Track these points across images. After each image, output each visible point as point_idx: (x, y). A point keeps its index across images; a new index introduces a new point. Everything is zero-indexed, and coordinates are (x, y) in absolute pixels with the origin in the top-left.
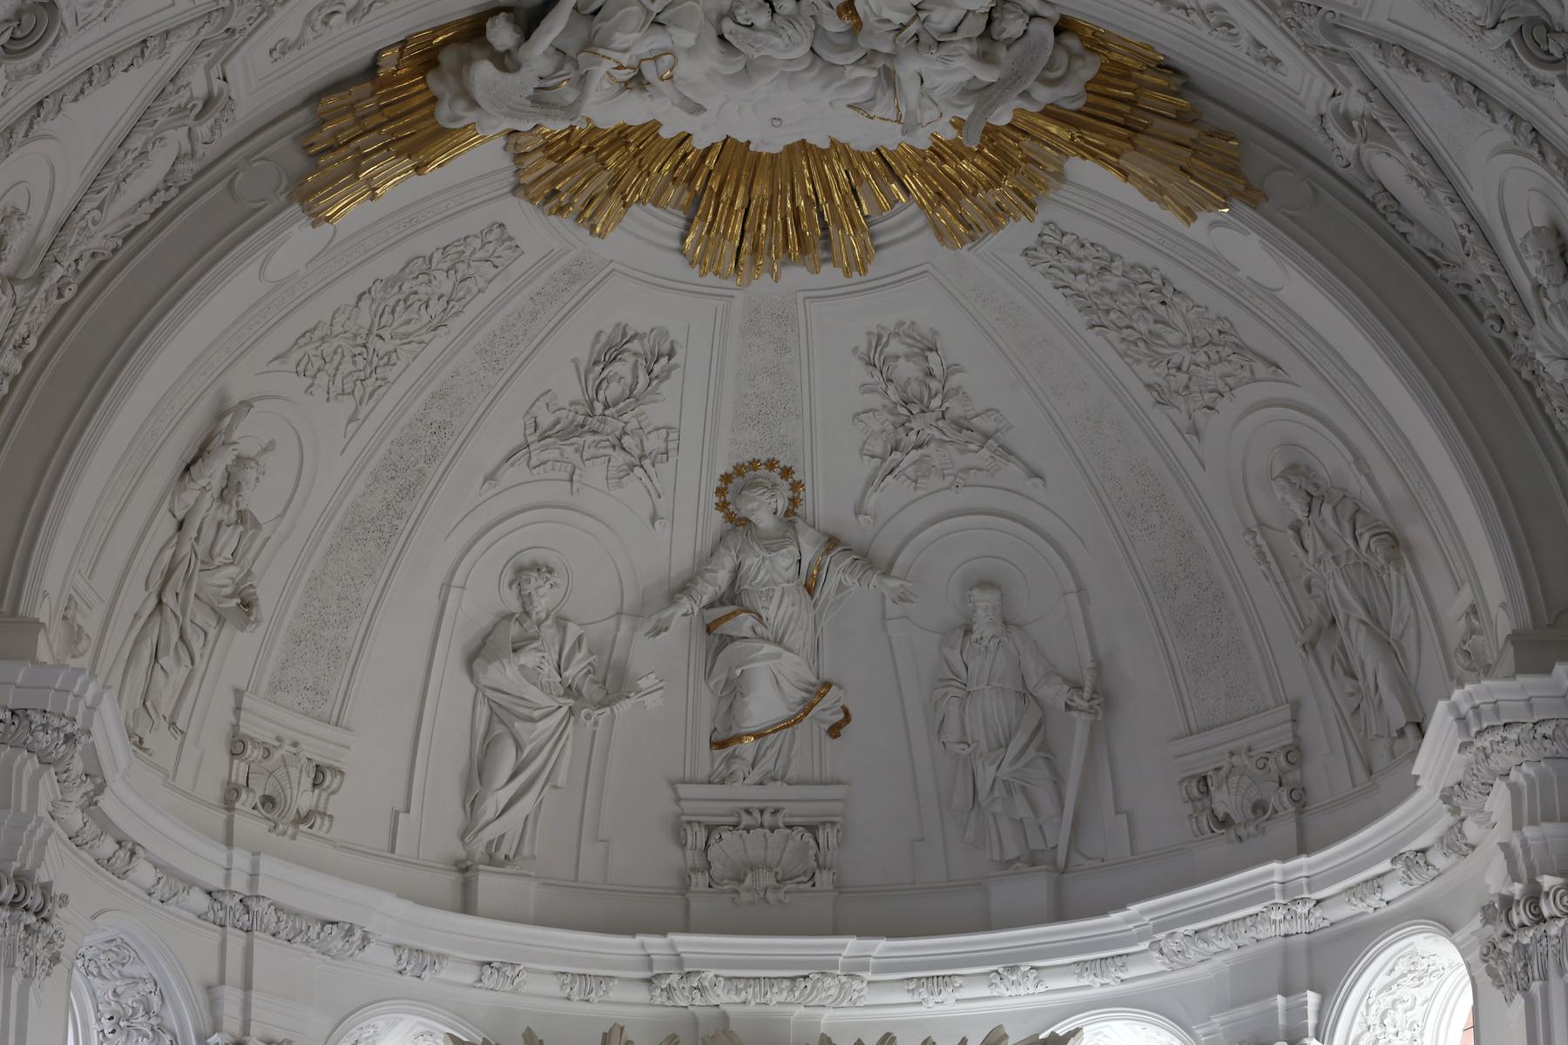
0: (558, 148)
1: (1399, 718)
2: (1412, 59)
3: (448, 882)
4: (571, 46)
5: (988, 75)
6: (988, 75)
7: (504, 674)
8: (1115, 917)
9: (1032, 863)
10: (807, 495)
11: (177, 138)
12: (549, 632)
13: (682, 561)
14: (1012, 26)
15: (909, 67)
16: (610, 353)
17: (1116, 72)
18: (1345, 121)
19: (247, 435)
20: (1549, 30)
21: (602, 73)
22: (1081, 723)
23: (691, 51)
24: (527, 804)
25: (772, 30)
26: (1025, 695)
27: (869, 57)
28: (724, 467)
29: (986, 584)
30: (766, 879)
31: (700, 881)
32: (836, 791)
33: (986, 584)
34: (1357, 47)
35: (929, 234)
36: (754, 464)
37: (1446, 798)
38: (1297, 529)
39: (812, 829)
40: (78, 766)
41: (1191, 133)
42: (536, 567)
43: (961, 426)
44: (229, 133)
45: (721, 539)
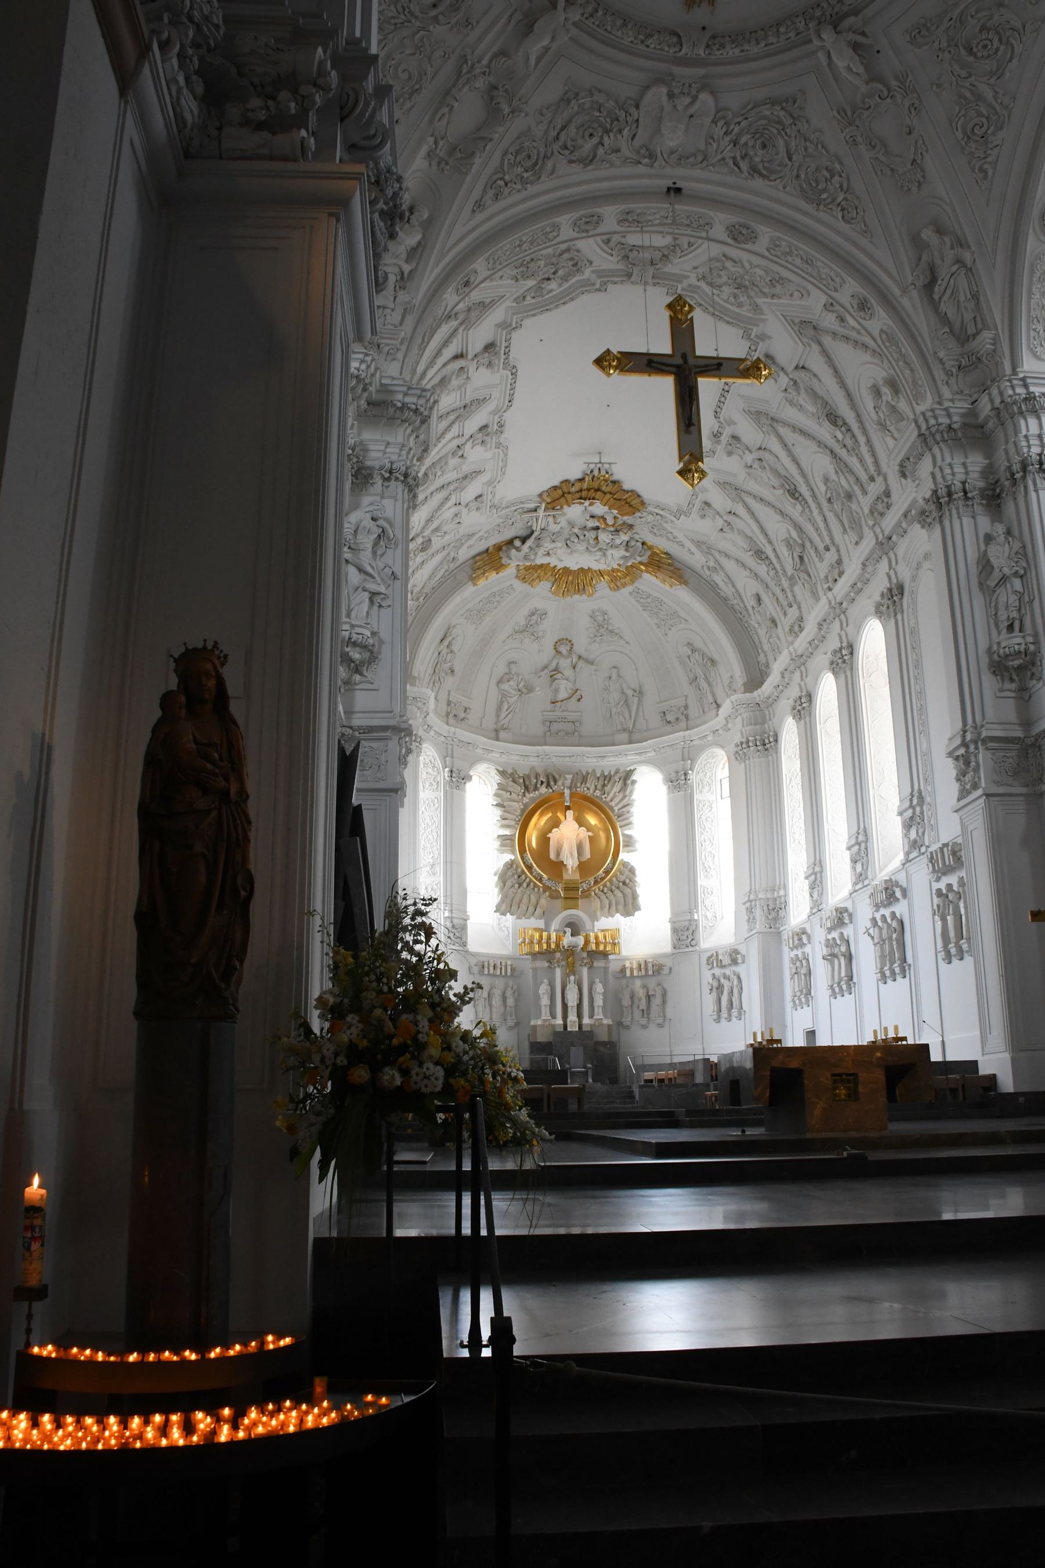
0: (527, 569)
1: (711, 700)
2: (727, 555)
4: (533, 546)
5: (628, 554)
6: (628, 554)
7: (505, 686)
8: (644, 743)
9: (624, 730)
10: (574, 647)
11: (446, 567)
12: (515, 677)
13: (545, 662)
14: (633, 543)
15: (609, 552)
16: (533, 614)
17: (654, 554)
18: (708, 568)
19: (455, 632)
20: (762, 552)
21: (541, 551)
22: (636, 700)
23: (560, 548)
24: (509, 717)
25: (578, 543)
26: (623, 693)
27: (600, 550)
28: (556, 640)
29: (615, 667)
30: (563, 734)
31: (548, 733)
32: (579, 714)
33: (615, 667)
34: (713, 552)
35: (608, 589)
36: (563, 639)
37: (726, 719)
38: (689, 657)
39: (573, 722)
40: (425, 710)
41: (671, 568)
42: (513, 662)
43: (611, 631)
44: (457, 565)
45: (554, 657)
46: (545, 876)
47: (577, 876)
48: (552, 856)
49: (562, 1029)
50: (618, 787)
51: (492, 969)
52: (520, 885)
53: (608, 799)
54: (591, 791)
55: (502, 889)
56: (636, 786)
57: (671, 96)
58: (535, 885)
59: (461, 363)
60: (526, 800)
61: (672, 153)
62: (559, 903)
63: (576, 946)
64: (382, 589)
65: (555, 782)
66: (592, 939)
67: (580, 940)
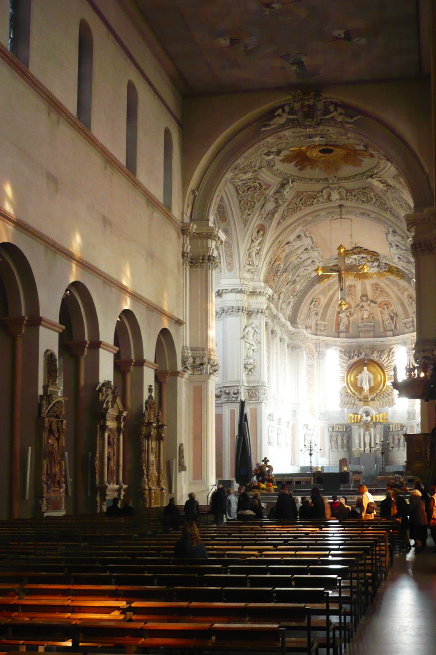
3: (337, 334)
7: (341, 315)
9: (392, 330)
17: (391, 267)
26: (390, 315)
29: (386, 305)
39: (371, 327)
46: (357, 393)
47: (368, 393)
48: (359, 385)
49: (363, 452)
50: (386, 355)
51: (337, 430)
52: (347, 396)
53: (382, 361)
54: (375, 358)
55: (341, 398)
56: (394, 354)
57: (331, 189)
58: (353, 397)
59: (289, 244)
60: (349, 363)
61: (337, 199)
62: (362, 402)
63: (367, 421)
64: (256, 347)
65: (361, 354)
66: (374, 418)
67: (369, 418)
